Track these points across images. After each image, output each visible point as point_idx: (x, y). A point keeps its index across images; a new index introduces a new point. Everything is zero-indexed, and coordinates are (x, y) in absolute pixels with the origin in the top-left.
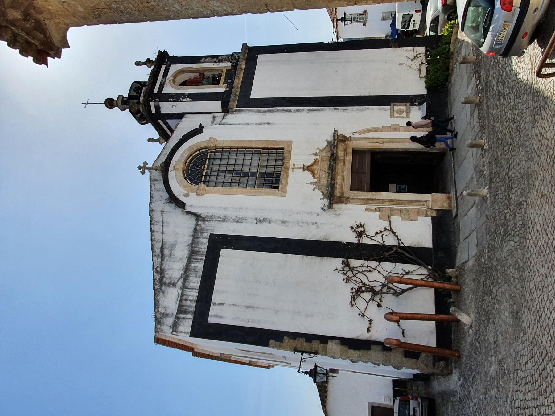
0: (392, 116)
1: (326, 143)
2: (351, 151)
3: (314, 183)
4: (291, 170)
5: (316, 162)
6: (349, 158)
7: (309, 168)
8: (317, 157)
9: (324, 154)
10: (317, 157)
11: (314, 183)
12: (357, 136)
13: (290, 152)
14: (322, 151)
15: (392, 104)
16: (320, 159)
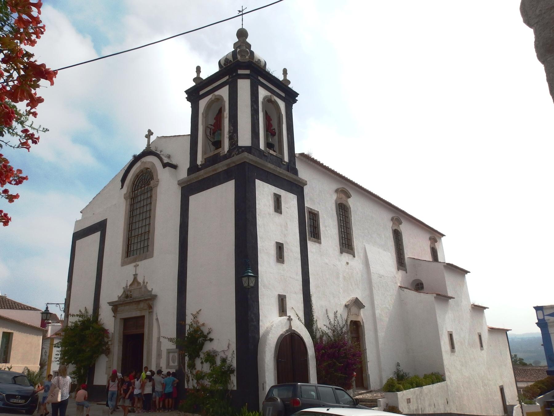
0: (169, 352)
1: (150, 289)
2: (143, 314)
3: (127, 287)
4: (134, 264)
5: (139, 283)
6: (137, 314)
7: (135, 279)
8: (142, 284)
9: (143, 289)
10: (142, 284)
11: (127, 287)
12: (155, 318)
13: (145, 258)
14: (146, 287)
15: (178, 350)
16: (140, 287)
